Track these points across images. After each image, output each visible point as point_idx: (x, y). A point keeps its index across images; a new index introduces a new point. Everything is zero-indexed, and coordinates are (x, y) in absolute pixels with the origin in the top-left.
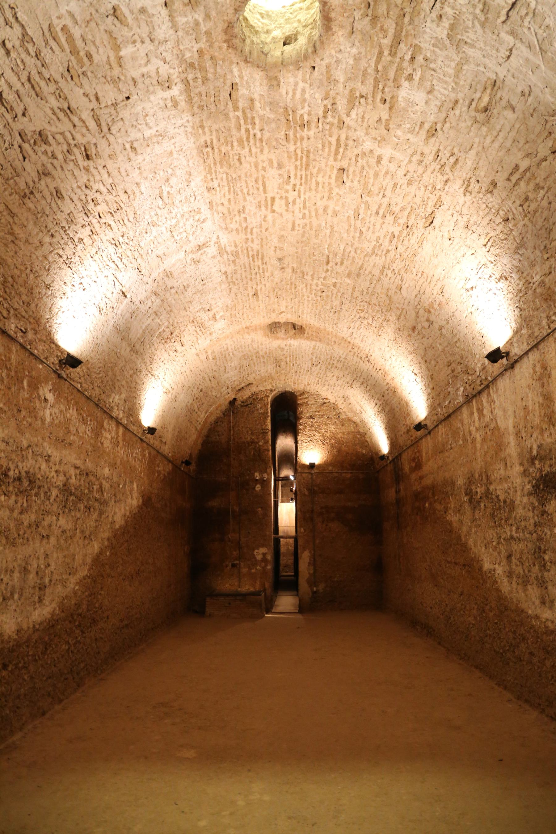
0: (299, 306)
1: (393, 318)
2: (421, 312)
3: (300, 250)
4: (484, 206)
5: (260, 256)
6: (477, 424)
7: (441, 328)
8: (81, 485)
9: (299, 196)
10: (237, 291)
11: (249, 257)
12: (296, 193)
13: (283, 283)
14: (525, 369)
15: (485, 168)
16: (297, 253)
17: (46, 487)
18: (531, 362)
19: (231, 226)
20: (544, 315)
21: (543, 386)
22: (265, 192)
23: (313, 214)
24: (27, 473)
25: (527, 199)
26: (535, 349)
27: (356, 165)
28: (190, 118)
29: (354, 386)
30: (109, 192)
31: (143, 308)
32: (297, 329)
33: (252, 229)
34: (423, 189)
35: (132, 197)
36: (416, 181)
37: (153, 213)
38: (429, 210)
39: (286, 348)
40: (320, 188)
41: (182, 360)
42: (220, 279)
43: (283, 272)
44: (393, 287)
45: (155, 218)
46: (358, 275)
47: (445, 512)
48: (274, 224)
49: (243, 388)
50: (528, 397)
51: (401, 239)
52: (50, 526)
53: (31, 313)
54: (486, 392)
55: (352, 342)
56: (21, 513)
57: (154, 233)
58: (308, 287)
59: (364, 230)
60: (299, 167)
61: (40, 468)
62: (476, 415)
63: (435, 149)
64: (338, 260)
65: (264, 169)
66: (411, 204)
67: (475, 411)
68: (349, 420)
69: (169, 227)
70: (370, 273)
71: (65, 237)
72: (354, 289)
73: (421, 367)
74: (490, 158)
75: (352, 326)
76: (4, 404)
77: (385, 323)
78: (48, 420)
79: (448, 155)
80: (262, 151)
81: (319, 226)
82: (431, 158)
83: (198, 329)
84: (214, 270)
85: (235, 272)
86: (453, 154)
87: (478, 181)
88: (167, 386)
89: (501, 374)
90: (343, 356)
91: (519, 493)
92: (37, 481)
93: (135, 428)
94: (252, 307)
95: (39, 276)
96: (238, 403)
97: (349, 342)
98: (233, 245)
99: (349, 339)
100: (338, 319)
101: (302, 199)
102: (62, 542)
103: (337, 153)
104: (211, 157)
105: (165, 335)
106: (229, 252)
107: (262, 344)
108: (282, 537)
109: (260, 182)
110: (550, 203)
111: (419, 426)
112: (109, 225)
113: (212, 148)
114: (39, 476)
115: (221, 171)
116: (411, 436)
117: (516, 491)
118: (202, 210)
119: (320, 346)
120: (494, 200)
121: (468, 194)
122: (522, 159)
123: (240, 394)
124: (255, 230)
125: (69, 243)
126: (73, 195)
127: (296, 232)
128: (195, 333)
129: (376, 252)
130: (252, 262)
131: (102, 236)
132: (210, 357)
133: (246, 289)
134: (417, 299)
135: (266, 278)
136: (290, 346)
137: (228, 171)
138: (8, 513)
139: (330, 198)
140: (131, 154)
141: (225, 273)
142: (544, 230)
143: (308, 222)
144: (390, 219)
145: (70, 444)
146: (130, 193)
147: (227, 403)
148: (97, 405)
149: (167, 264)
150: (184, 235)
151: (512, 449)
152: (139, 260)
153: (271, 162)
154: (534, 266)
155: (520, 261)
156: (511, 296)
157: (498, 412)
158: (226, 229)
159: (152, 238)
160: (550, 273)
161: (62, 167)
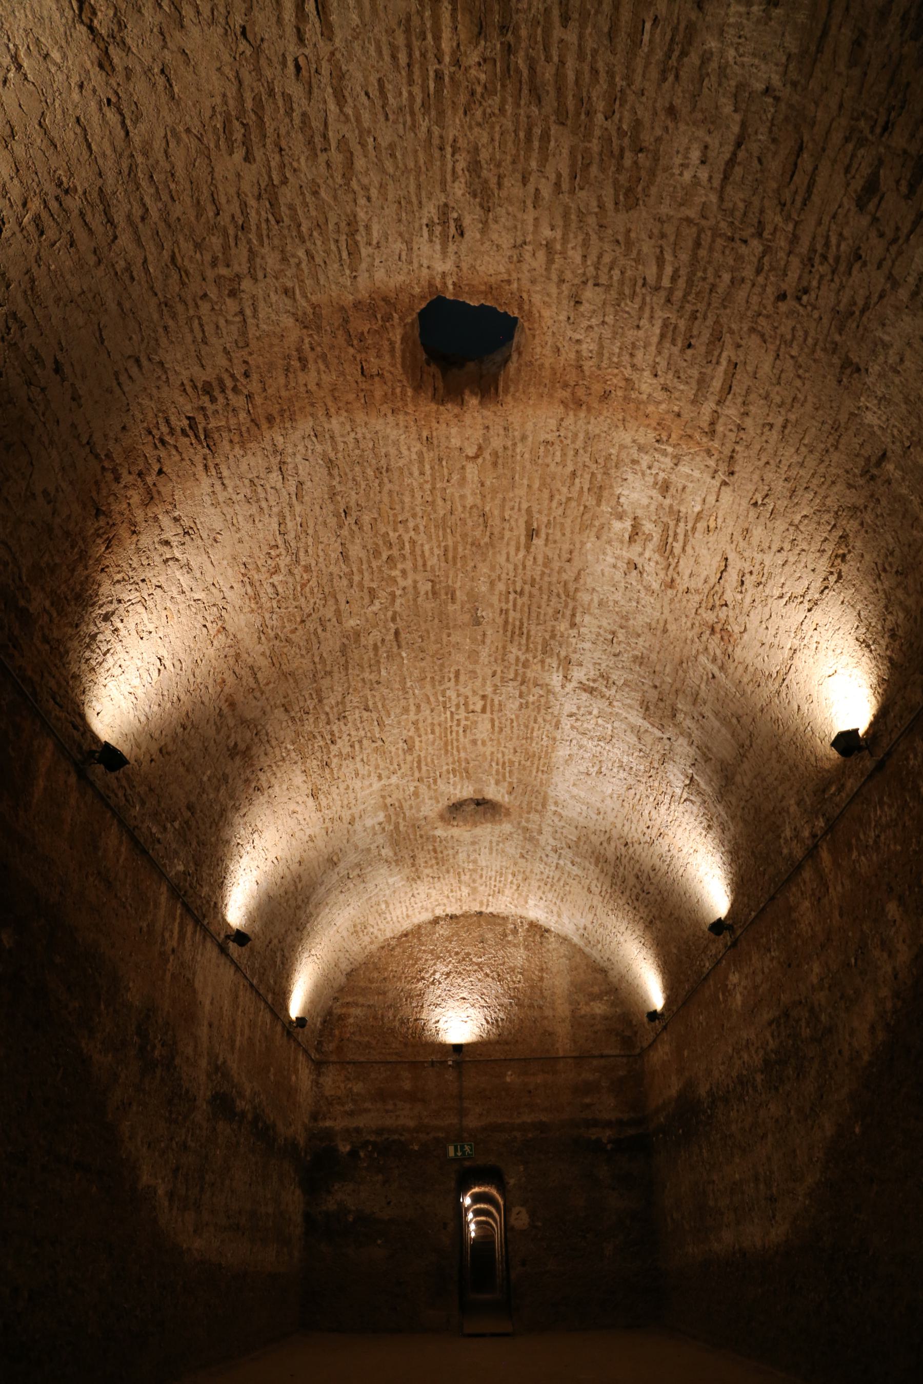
12: (456, 717)
23: (432, 699)
58: (420, 562)
59: (365, 714)
65: (491, 740)
72: (338, 612)
80: (492, 753)
94: (546, 494)
100: (333, 495)
103: (419, 762)
106: (555, 658)
109: (497, 729)
124: (512, 676)
130: (525, 620)
133: (547, 561)
135: (504, 576)
158: (549, 691)
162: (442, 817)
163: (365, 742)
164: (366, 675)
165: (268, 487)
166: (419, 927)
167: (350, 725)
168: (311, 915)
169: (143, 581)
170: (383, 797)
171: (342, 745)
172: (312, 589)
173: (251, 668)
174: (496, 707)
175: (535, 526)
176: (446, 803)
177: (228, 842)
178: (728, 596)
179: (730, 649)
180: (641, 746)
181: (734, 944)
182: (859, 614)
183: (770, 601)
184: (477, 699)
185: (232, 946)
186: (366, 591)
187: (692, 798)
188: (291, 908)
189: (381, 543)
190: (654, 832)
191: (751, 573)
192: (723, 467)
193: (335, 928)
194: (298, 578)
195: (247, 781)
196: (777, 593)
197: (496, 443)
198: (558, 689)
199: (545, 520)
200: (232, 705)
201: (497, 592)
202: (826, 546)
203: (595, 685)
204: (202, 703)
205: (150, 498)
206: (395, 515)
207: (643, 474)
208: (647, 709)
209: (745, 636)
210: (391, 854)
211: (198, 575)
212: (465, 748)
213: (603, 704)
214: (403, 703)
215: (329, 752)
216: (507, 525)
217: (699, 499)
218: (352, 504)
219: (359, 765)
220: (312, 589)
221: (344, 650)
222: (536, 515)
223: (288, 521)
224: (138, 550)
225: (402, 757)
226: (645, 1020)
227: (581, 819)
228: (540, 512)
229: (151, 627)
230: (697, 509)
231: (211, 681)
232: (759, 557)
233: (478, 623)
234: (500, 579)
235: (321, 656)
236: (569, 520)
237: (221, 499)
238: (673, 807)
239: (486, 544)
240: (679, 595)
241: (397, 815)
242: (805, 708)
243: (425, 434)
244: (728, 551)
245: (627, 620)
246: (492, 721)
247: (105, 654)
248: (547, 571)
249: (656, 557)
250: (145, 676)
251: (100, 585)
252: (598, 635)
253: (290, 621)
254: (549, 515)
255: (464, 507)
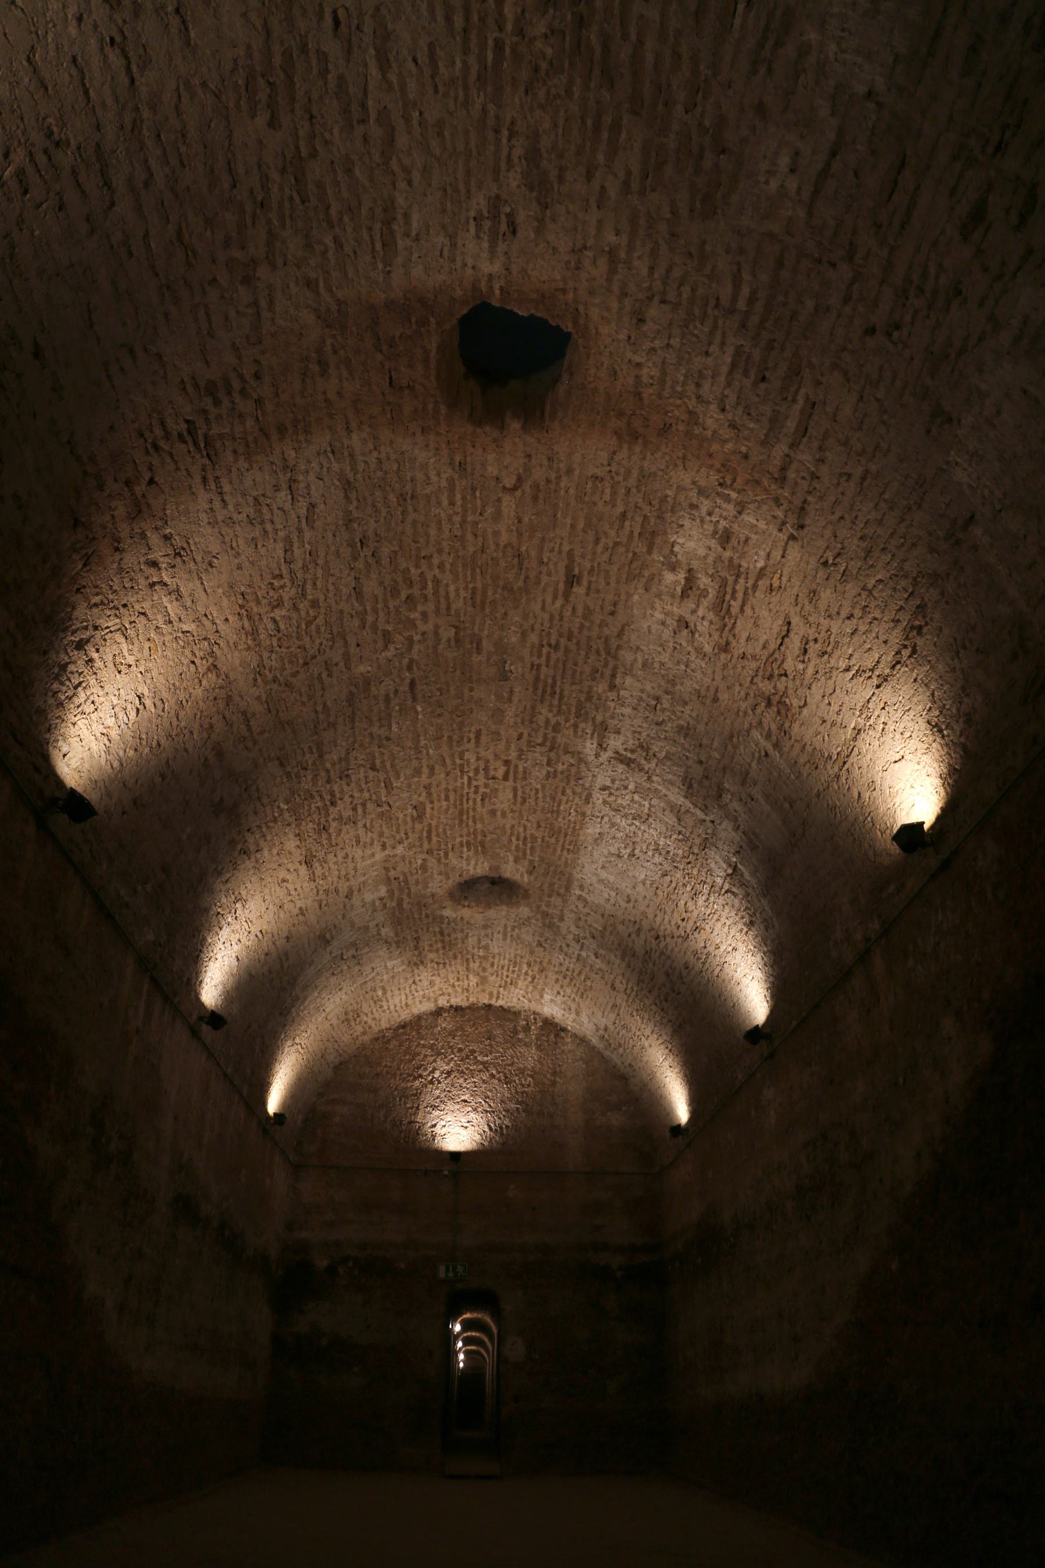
0: (464, 521)
9: (469, 778)
10: (610, 619)
12: (474, 783)
16: (471, 690)
23: (448, 761)
28: (575, 873)
58: (443, 605)
59: (371, 774)
72: (347, 656)
80: (513, 826)
81: (438, 747)
94: (591, 537)
98: (580, 729)
100: (349, 521)
103: (429, 832)
106: (590, 723)
109: (519, 799)
124: (540, 740)
127: (473, 729)
130: (559, 678)
133: (588, 614)
135: (537, 627)
139: (427, 787)
143: (456, 748)
153: (504, 814)
158: (580, 760)
162: (451, 895)
163: (369, 805)
164: (375, 730)
165: (274, 507)
166: (419, 1018)
167: (353, 785)
168: (297, 998)
169: (125, 606)
170: (387, 869)
171: (343, 808)
172: (318, 628)
173: (244, 713)
174: (520, 775)
175: (576, 571)
176: (458, 879)
177: (207, 910)
178: (789, 665)
179: (787, 725)
180: (680, 828)
181: (771, 1056)
182: (933, 694)
183: (835, 673)
184: (499, 763)
185: (205, 1028)
186: (380, 633)
187: (734, 889)
188: (274, 988)
189: (400, 579)
190: (690, 925)
191: (816, 640)
192: (792, 519)
193: (324, 1015)
194: (303, 614)
195: (232, 843)
196: (843, 665)
197: (538, 474)
198: (591, 758)
199: (588, 565)
200: (220, 754)
201: (528, 645)
202: (901, 616)
203: (633, 757)
204: (186, 750)
205: (138, 510)
206: (418, 549)
207: (702, 521)
208: (690, 786)
209: (805, 711)
210: (392, 934)
211: (189, 604)
212: (482, 819)
213: (641, 778)
214: (415, 763)
215: (327, 815)
216: (545, 569)
217: (762, 553)
218: (370, 533)
219: (361, 831)
220: (318, 628)
221: (351, 699)
222: (578, 560)
223: (295, 548)
224: (120, 570)
226: (668, 1134)
227: (608, 907)
228: (583, 556)
229: (131, 660)
230: (760, 564)
231: (196, 726)
232: (825, 623)
233: (505, 678)
234: (533, 629)
235: (325, 705)
236: (615, 568)
237: (220, 518)
238: (712, 899)
239: (520, 589)
240: (734, 661)
241: (401, 890)
242: (866, 795)
243: (458, 458)
244: (792, 614)
245: (674, 685)
246: (515, 790)
247: (76, 688)
248: (587, 624)
249: (711, 616)
250: (121, 715)
251: (74, 608)
252: (640, 699)
253: (291, 662)
254: (592, 561)
255: (497, 545)
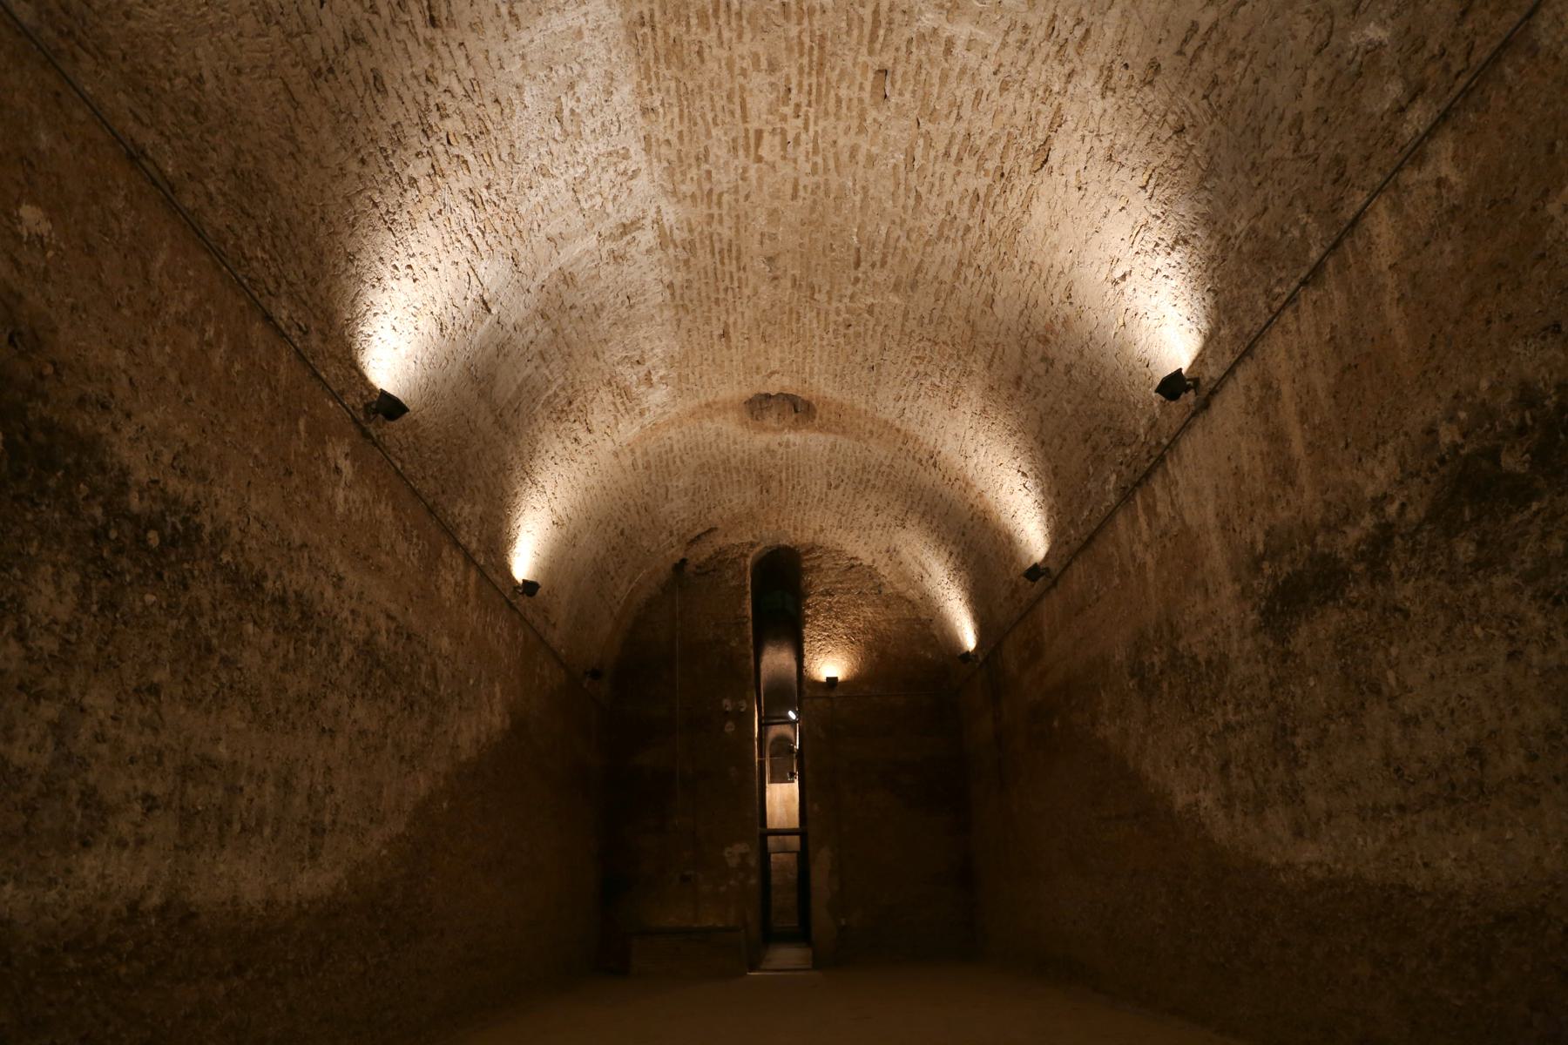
1: (978, 367)
2: (1032, 344)
3: (806, 240)
4: (1139, 111)
5: (734, 254)
6: (1145, 537)
7: (1069, 369)
8: (396, 653)
9: (806, 128)
10: (690, 326)
11: (713, 254)
12: (800, 122)
13: (776, 310)
14: (1231, 404)
15: (1138, 39)
16: (801, 245)
17: (332, 633)
18: (1242, 383)
19: (683, 188)
20: (1259, 291)
21: (1267, 417)
22: (745, 119)
23: (832, 164)
24: (298, 595)
25: (1215, 83)
26: (1247, 359)
27: (907, 61)
29: (908, 525)
30: (467, 95)
31: (520, 341)
32: (799, 409)
33: (720, 195)
34: (1027, 96)
35: (507, 111)
36: (1015, 81)
37: (543, 150)
38: (1041, 136)
39: (781, 450)
40: (844, 110)
41: (587, 463)
42: (660, 299)
43: (776, 287)
44: (978, 302)
45: (546, 160)
46: (914, 286)
47: (1093, 725)
48: (760, 187)
49: (699, 537)
50: (1239, 449)
51: (991, 201)
52: (337, 713)
53: (318, 300)
54: (1160, 470)
55: (903, 428)
56: (284, 669)
57: (545, 190)
58: (822, 316)
59: (923, 190)
60: (807, 70)
61: (322, 594)
62: (1143, 520)
63: (1048, 15)
64: (877, 257)
65: (744, 73)
66: (1008, 128)
67: (1140, 511)
68: (900, 597)
69: (570, 180)
70: (936, 277)
71: (386, 170)
72: (906, 315)
73: (1033, 457)
74: (1147, 17)
75: (903, 393)
76: (262, 450)
77: (964, 380)
78: (340, 509)
79: (1070, 23)
80: (740, 37)
81: (842, 187)
82: (1041, 33)
83: (618, 401)
84: (650, 277)
85: (688, 284)
86: (1079, 22)
87: (1126, 66)
88: (559, 509)
89: (1186, 427)
90: (887, 462)
91: (1235, 636)
92: (316, 617)
93: (499, 579)
94: (718, 361)
95: (335, 233)
96: (690, 568)
97: (898, 430)
99: (898, 422)
100: (877, 382)
101: (811, 133)
102: (360, 752)
103: (873, 37)
104: (650, 46)
105: (561, 402)
107: (735, 443)
108: (777, 832)
109: (737, 100)
110: (1257, 81)
111: (1035, 572)
112: (465, 162)
113: (653, 28)
114: (320, 608)
115: (668, 73)
116: (1020, 601)
117: (1230, 635)
118: (632, 152)
119: (845, 443)
120: (1154, 98)
121: (1109, 93)
122: (1203, 9)
123: (695, 549)
124: (726, 197)
125: (393, 182)
126: (403, 90)
128: (612, 408)
129: (946, 232)
131: (451, 179)
132: (640, 462)
133: (708, 322)
134: (1024, 320)
136: (787, 446)
137: (680, 75)
138: (258, 659)
139: (861, 130)
140: (508, 26)
141: (671, 286)
142: (1249, 134)
144: (969, 163)
145: (380, 569)
146: (504, 103)
147: (669, 567)
148: (431, 511)
149: (566, 256)
150: (598, 200)
151: (1217, 556)
152: (516, 242)
154: (1234, 204)
155: (1209, 201)
156: (1195, 272)
157: (1186, 499)
158: (674, 193)
159: (540, 199)
160: (1266, 209)
161: (386, 32)
198: (663, 203)
225: (900, 70)
